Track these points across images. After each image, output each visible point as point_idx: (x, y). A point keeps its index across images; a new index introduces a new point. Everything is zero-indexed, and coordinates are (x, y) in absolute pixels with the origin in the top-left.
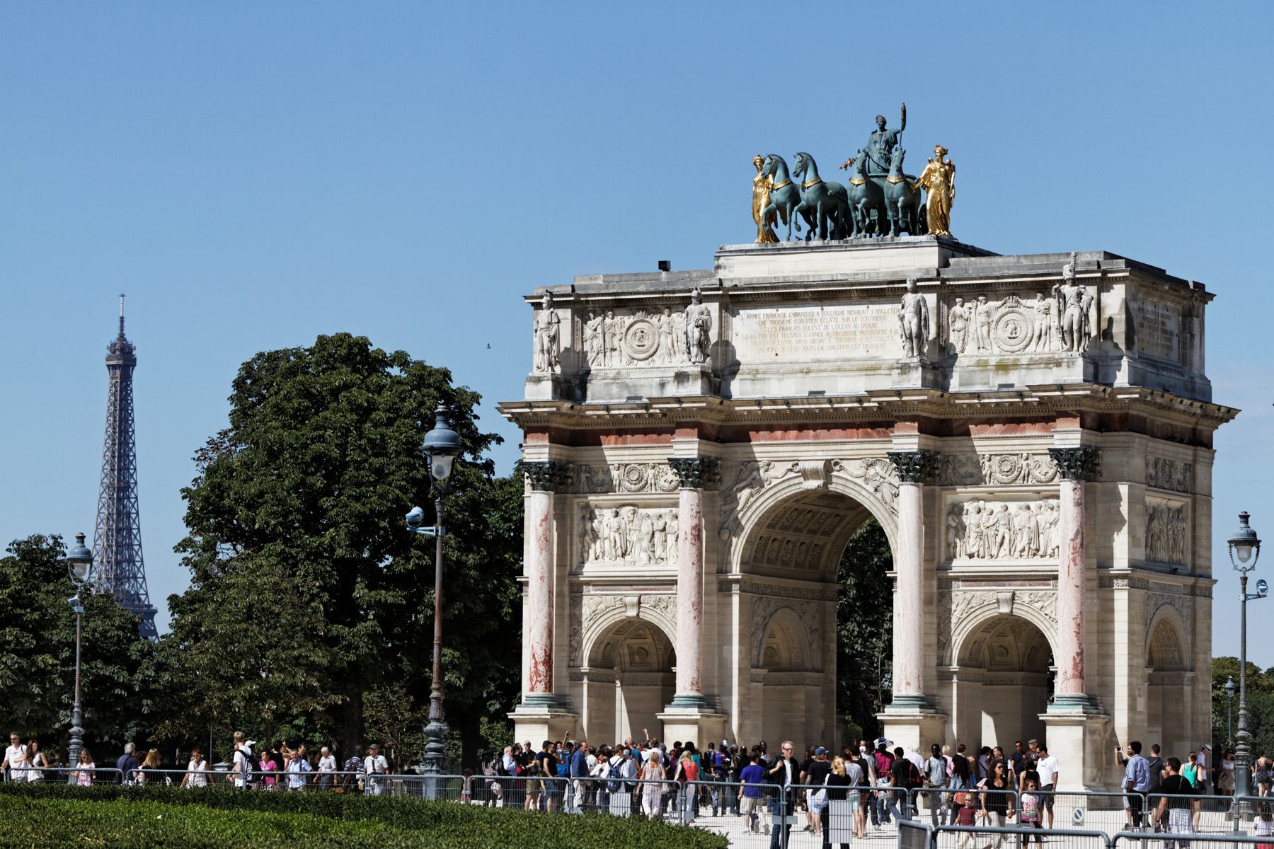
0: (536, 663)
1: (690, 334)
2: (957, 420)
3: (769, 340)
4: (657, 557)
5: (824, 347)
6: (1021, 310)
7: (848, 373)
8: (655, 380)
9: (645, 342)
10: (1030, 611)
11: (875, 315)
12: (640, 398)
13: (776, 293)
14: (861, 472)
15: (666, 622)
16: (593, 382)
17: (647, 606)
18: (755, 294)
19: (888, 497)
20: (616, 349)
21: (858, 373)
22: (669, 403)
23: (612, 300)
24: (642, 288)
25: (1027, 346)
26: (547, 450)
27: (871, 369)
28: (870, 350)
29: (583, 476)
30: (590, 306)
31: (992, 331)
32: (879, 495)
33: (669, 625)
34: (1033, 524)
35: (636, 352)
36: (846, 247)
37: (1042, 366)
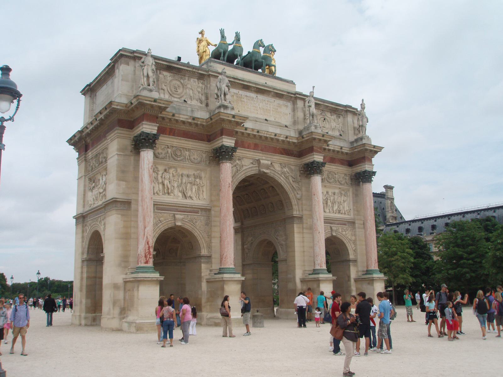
0: (149, 247)
1: (223, 89)
3: (235, 104)
4: (189, 195)
7: (273, 126)
9: (178, 90)
10: (342, 236)
13: (242, 84)
15: (196, 229)
17: (186, 220)
18: (233, 82)
19: (291, 181)
21: (276, 127)
22: (229, 117)
23: (166, 65)
27: (280, 126)
28: (276, 119)
33: (198, 231)
35: (173, 93)
37: (339, 140)
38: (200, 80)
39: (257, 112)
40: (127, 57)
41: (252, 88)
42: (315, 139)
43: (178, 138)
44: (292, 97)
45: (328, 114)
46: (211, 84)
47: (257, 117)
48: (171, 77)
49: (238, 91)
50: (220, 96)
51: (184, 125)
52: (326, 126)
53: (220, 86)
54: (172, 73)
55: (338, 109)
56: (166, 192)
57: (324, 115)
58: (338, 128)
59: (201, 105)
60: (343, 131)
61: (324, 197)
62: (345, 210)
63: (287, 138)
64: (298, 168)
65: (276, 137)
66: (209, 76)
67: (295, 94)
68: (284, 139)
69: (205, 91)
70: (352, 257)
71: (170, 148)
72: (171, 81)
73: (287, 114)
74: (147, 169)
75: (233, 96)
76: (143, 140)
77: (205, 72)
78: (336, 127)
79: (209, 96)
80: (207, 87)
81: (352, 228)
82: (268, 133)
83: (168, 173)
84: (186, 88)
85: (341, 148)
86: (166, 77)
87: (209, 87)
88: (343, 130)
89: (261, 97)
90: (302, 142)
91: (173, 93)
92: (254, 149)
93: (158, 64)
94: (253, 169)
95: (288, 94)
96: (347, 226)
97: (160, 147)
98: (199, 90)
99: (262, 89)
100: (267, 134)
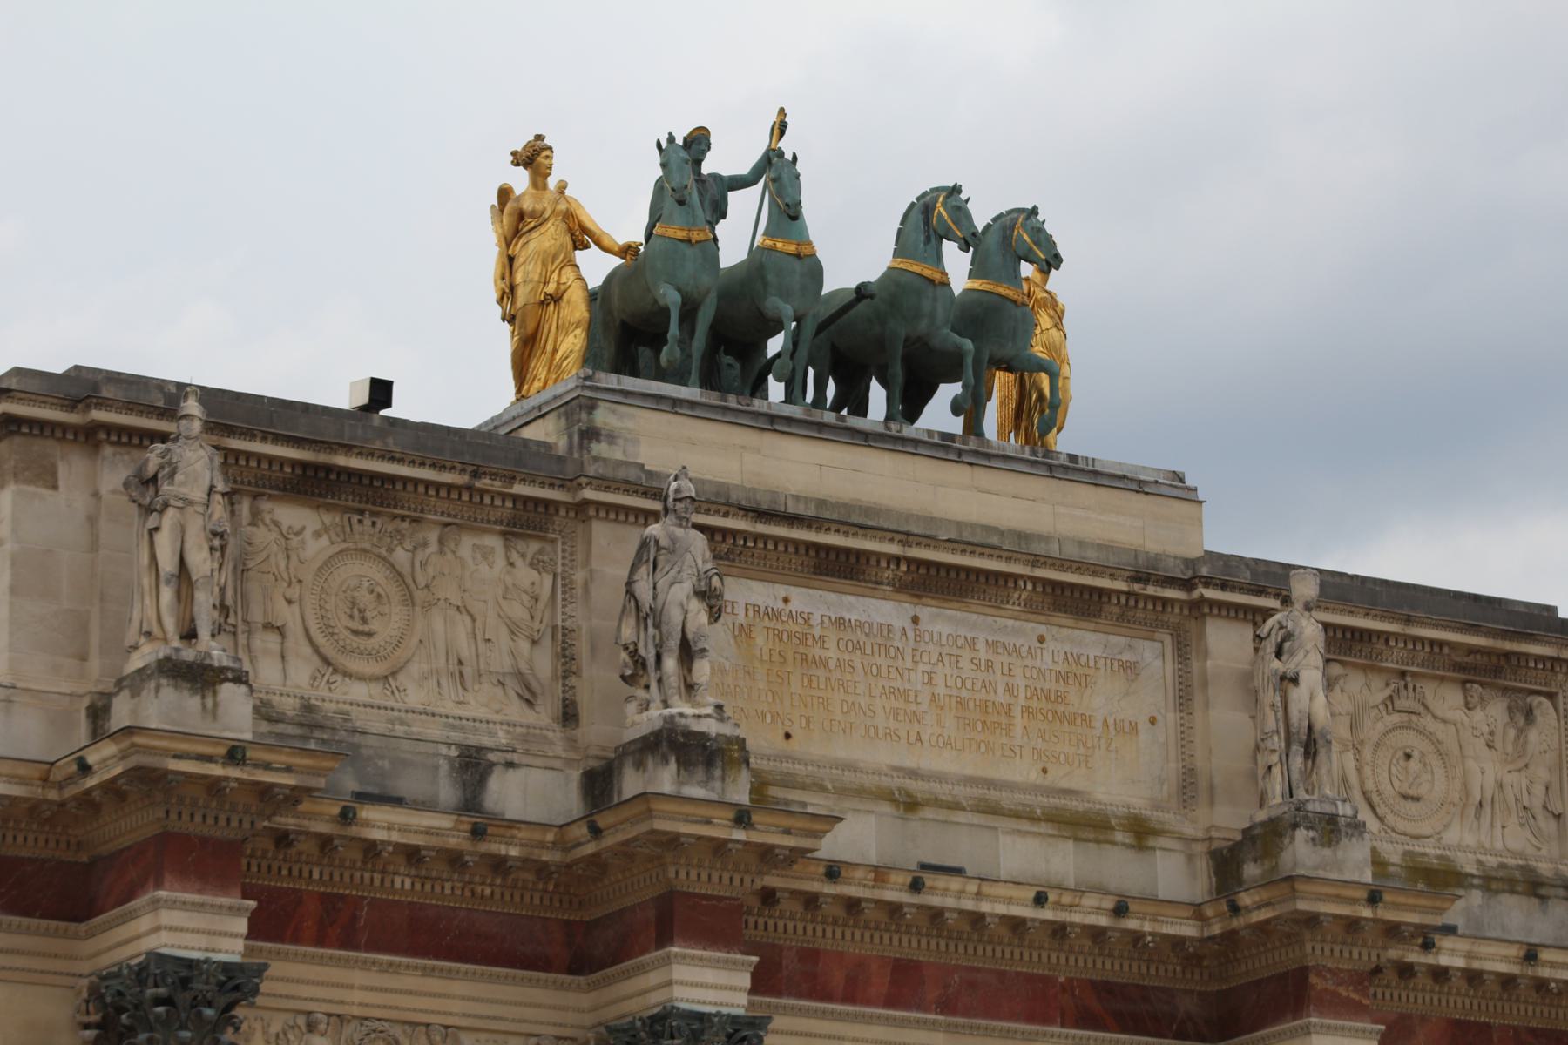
1: (675, 616)
3: (762, 685)
5: (925, 738)
6: (1427, 722)
7: (1025, 826)
8: (444, 750)
9: (374, 625)
11: (1062, 667)
13: (809, 546)
18: (745, 535)
20: (281, 631)
22: (708, 822)
23: (294, 463)
25: (1446, 826)
26: (242, 925)
31: (1368, 771)
35: (344, 650)
38: (520, 545)
39: (916, 727)
40: (42, 430)
41: (884, 564)
42: (1312, 920)
43: (374, 963)
44: (1165, 602)
45: (1446, 700)
46: (595, 565)
47: (910, 763)
48: (324, 541)
49: (782, 590)
50: (651, 661)
51: (413, 872)
52: (1421, 791)
53: (655, 598)
54: (329, 508)
55: (1519, 655)
57: (1418, 707)
59: (530, 717)
60: (1558, 817)
63: (1120, 910)
65: (1047, 914)
66: (582, 509)
67: (1187, 585)
68: (1103, 921)
69: (553, 616)
71: (322, 1027)
72: (329, 563)
73: (1134, 728)
75: (748, 636)
76: (160, 1009)
77: (552, 485)
78: (1501, 786)
79: (583, 648)
80: (568, 586)
82: (987, 888)
84: (428, 606)
85: (1531, 956)
86: (295, 541)
87: (579, 591)
88: (1558, 809)
90: (1230, 936)
91: (344, 650)
92: (890, 1003)
93: (242, 462)
95: (1137, 587)
97: (258, 1026)
98: (518, 611)
99: (949, 567)
100: (979, 895)
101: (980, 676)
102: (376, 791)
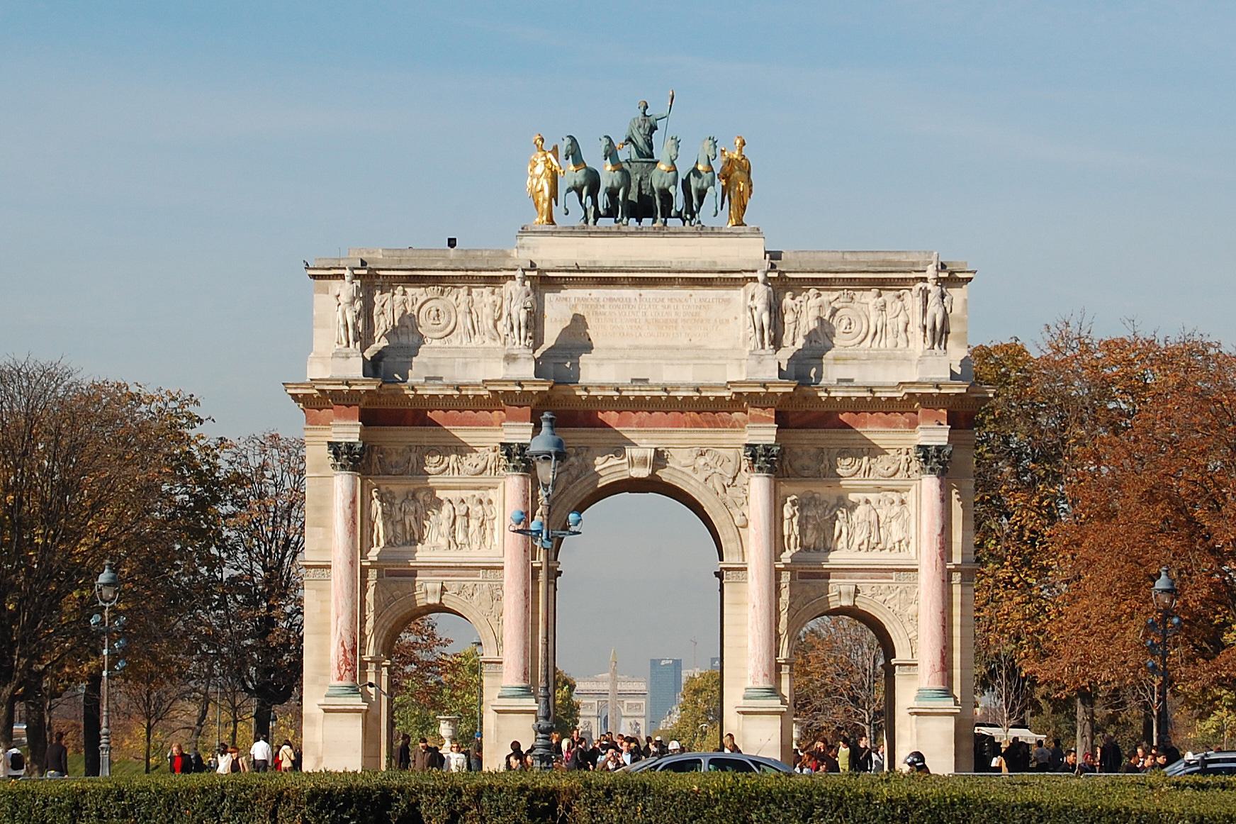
0: (345, 650)
1: (514, 316)
2: (794, 412)
6: (856, 305)
10: (872, 604)
11: (698, 304)
12: (441, 379)
14: (688, 462)
16: (385, 359)
21: (685, 362)
22: (506, 385)
23: (406, 276)
24: (440, 265)
29: (375, 457)
30: (378, 282)
32: (710, 485)
33: (475, 613)
34: (873, 517)
36: (664, 234)
47: (637, 343)
49: (588, 291)
56: (408, 538)
58: (893, 329)
59: (493, 344)
61: (827, 512)
62: (896, 539)
64: (742, 451)
68: (691, 394)
70: (901, 655)
73: (727, 321)
74: (342, 510)
81: (909, 585)
83: (412, 502)
89: (649, 293)
94: (613, 470)
95: (722, 275)
96: (894, 581)
98: (488, 310)
101: (665, 311)
102: (432, 376)
